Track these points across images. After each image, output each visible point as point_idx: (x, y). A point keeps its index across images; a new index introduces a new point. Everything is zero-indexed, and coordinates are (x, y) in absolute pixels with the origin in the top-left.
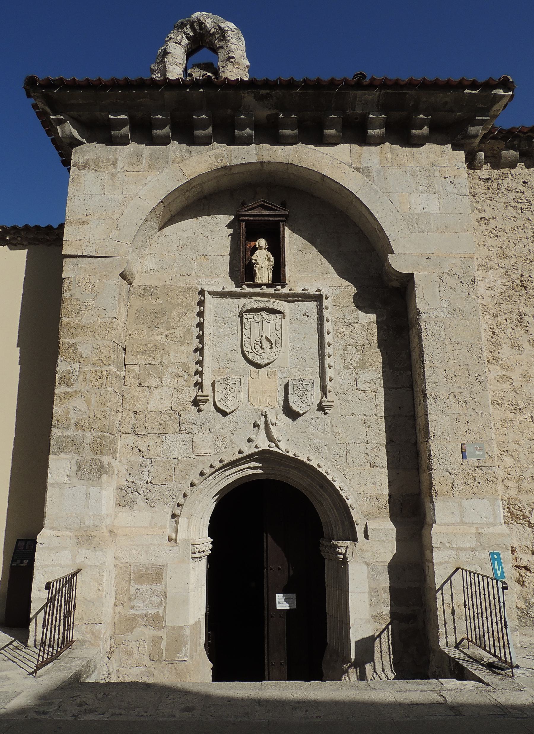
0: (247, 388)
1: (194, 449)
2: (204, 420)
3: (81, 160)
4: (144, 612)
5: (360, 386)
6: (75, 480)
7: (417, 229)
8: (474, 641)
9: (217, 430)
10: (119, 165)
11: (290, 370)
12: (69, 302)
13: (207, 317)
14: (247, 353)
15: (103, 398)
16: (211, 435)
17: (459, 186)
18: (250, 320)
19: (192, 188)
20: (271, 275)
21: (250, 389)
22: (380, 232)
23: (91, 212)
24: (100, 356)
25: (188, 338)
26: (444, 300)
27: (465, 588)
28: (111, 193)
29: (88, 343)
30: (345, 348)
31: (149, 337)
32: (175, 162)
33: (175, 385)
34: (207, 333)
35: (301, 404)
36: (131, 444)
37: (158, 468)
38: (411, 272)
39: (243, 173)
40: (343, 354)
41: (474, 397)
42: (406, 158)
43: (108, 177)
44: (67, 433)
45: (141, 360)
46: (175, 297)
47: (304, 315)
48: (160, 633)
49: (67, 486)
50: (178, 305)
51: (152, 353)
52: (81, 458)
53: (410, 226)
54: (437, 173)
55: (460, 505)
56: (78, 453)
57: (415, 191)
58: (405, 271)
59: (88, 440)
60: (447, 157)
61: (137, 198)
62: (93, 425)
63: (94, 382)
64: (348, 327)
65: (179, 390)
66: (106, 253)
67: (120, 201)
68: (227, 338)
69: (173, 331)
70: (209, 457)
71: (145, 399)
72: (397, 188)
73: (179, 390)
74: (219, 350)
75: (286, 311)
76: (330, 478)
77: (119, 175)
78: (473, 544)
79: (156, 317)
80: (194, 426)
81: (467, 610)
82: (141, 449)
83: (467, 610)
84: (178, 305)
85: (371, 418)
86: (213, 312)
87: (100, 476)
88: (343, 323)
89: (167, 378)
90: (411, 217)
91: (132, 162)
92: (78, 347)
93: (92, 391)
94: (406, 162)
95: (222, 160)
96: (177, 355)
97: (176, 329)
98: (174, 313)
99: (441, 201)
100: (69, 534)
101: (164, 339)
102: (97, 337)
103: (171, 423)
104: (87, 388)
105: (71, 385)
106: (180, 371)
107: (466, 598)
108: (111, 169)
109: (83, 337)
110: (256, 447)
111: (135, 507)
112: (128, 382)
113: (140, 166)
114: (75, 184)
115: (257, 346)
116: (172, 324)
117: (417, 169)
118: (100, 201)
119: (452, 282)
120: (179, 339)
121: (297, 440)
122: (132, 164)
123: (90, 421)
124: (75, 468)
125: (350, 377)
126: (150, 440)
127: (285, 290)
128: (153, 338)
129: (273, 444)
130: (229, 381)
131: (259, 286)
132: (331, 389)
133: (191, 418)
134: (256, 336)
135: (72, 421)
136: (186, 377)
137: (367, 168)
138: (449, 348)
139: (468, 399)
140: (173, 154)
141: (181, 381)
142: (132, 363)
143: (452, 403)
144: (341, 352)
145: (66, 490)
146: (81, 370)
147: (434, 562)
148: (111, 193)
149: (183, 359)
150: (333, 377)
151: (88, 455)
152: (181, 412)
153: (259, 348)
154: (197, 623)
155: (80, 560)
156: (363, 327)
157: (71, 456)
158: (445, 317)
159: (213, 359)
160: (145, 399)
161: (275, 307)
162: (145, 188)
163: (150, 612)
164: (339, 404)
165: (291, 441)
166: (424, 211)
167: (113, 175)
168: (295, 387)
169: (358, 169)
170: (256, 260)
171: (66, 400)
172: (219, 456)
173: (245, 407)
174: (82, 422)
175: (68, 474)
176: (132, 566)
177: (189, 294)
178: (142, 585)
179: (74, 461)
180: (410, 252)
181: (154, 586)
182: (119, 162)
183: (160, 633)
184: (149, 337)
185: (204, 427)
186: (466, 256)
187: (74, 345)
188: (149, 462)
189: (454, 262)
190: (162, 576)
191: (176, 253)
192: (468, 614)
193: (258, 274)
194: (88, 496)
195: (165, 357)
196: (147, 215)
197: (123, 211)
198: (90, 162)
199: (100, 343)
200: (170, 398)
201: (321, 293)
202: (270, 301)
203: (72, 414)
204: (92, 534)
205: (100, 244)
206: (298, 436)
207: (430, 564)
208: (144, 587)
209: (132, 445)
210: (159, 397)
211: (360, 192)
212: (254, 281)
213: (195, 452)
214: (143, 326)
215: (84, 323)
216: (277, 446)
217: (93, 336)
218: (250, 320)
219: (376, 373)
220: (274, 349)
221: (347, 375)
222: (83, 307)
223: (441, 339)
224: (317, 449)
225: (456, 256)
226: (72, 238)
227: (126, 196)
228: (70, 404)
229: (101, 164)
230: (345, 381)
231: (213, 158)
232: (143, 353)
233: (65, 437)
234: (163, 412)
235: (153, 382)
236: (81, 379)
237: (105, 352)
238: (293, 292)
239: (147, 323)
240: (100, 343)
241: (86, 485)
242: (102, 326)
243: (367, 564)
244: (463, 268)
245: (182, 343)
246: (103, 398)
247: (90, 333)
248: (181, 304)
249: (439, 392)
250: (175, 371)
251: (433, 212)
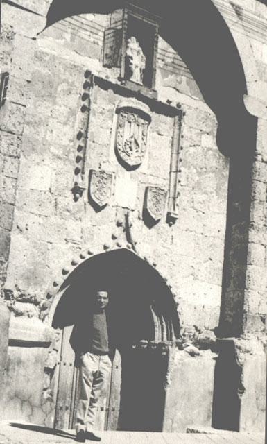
14: (119, 152)
38: (256, 115)
82: (20, 226)
110: (118, 245)
129: (130, 245)
134: (127, 137)
165: (147, 245)
216: (133, 248)
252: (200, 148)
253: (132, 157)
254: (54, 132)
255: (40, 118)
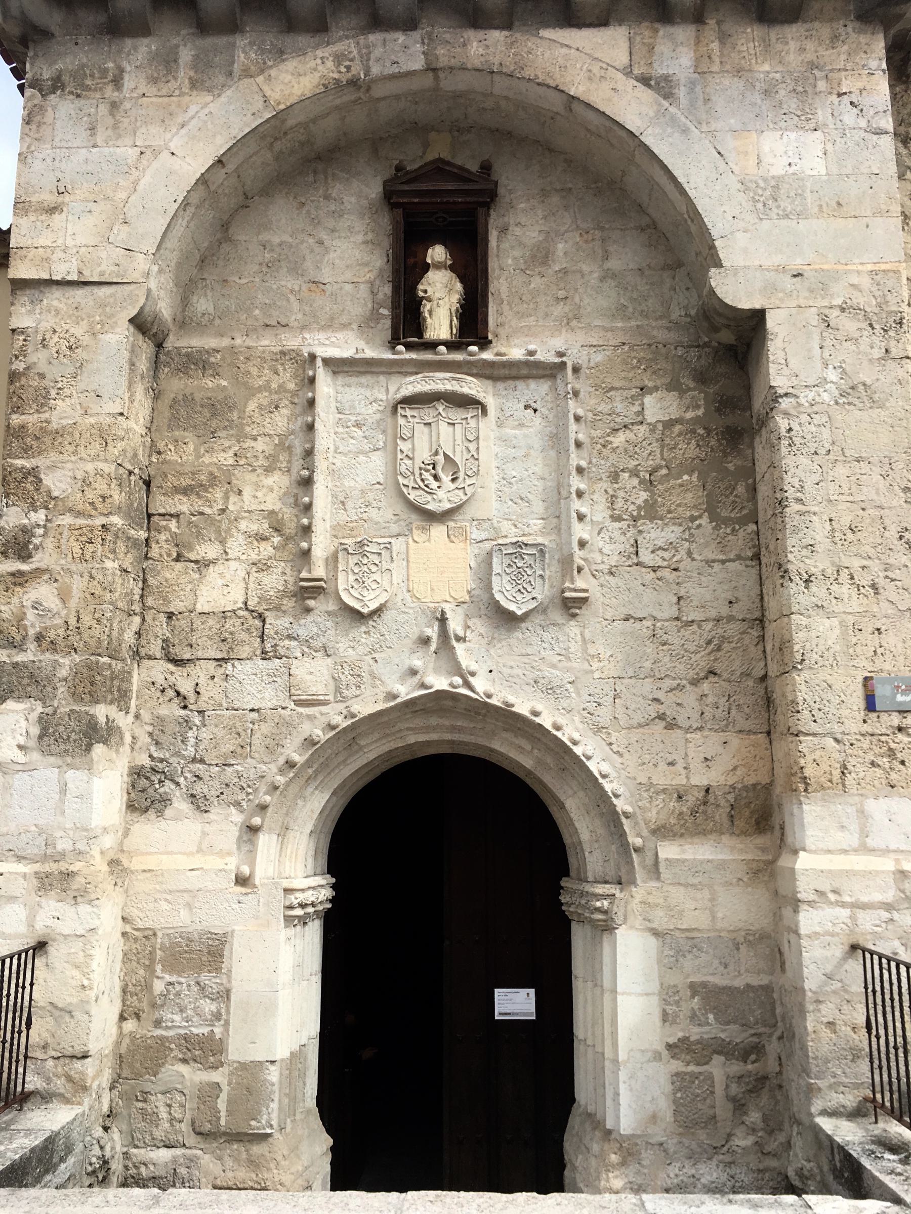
0: (405, 563)
1: (293, 691)
2: (315, 630)
3: (47, 74)
4: (182, 1032)
5: (646, 557)
6: (35, 756)
7: (775, 210)
8: (888, 1104)
9: (341, 650)
10: (128, 82)
11: (496, 525)
12: (23, 381)
13: (322, 414)
14: (405, 490)
15: (96, 583)
16: (329, 661)
17: (872, 112)
18: (410, 419)
19: (285, 133)
20: (455, 321)
21: (411, 565)
22: (692, 221)
23: (69, 187)
24: (90, 495)
25: (281, 458)
26: (831, 367)
27: (870, 990)
28: (111, 143)
29: (63, 468)
30: (615, 477)
31: (198, 456)
32: (247, 73)
33: (254, 557)
34: (321, 448)
35: (519, 597)
36: (160, 680)
37: (216, 730)
38: (758, 307)
39: (397, 97)
40: (609, 490)
41: (894, 576)
42: (753, 52)
43: (103, 109)
44: (20, 658)
45: (183, 505)
46: (254, 371)
47: (526, 407)
48: (216, 1076)
49: (19, 767)
50: (260, 389)
51: (206, 491)
52: (49, 710)
53: (760, 206)
54: (822, 85)
55: (861, 812)
56: (43, 700)
57: (771, 126)
58: (745, 304)
59: (63, 672)
60: (846, 47)
61: (166, 154)
62: (74, 640)
63: (77, 550)
64: (621, 433)
65: (261, 566)
66: (102, 274)
67: (129, 161)
68: (362, 458)
69: (249, 443)
70: (323, 709)
71: (190, 586)
72: (732, 121)
73: (261, 566)
74: (347, 484)
75: (490, 401)
76: (578, 750)
77: (127, 105)
78: (889, 896)
79: (214, 415)
80: (294, 643)
81: (874, 1039)
82: (182, 690)
83: (874, 1039)
84: (260, 389)
85: (666, 624)
86: (333, 405)
87: (89, 748)
88: (612, 425)
89: (236, 545)
90: (762, 184)
91: (155, 75)
92: (42, 476)
93: (73, 568)
94: (754, 61)
95: (348, 68)
96: (259, 494)
97: (256, 440)
98: (252, 406)
99: (829, 147)
100: (21, 868)
101: (231, 461)
102: (85, 457)
103: (244, 636)
104: (63, 562)
105: (30, 556)
106: (264, 527)
107: (872, 1012)
108: (109, 91)
109: (53, 456)
110: (423, 686)
111: (168, 812)
112: (155, 551)
113: (173, 84)
114: (34, 127)
115: (426, 475)
116: (248, 429)
117: (778, 76)
118: (86, 161)
119: (849, 325)
120: (262, 461)
121: (509, 671)
122: (154, 80)
123: (69, 632)
124: (35, 731)
125: (623, 539)
126: (201, 672)
127: (487, 355)
128: (207, 459)
129: (458, 680)
130: (366, 548)
131: (432, 346)
132: (582, 563)
133: (287, 625)
134: (423, 454)
135: (32, 632)
136: (277, 540)
137: (666, 78)
138: (841, 471)
139: (881, 582)
140: (242, 55)
141: (267, 549)
142: (162, 511)
143: (845, 590)
144: (605, 485)
145: (17, 776)
146: (49, 525)
147: (803, 931)
148: (111, 143)
149: (272, 502)
150: (586, 536)
151: (63, 703)
152: (267, 613)
153: (431, 478)
154: (297, 1056)
155: (43, 923)
156: (653, 430)
157: (28, 705)
158: (832, 403)
159: (334, 504)
160: (190, 586)
161: (466, 390)
162: (183, 131)
163: (195, 1031)
164: (599, 595)
166: (791, 170)
167: (114, 106)
168: (507, 561)
169: (645, 81)
170: (425, 292)
171: (18, 589)
172: (345, 705)
173: (400, 603)
174: (52, 635)
175: (22, 743)
176: (159, 934)
177: (282, 364)
178: (179, 973)
179: (34, 716)
180: (757, 263)
181: (205, 978)
182: (126, 77)
183: (216, 1076)
184: (198, 456)
185: (314, 644)
186: (883, 267)
187: (34, 473)
188: (197, 720)
189: (855, 280)
190: (222, 956)
191: (257, 279)
192: (875, 1046)
193: (429, 321)
194: (64, 791)
195: (233, 498)
196: (188, 192)
197: (136, 183)
198: (66, 78)
199: (90, 467)
200: (243, 585)
201: (564, 359)
202: (454, 379)
203: (31, 615)
204: (72, 868)
205: (89, 256)
206: (512, 663)
207: (792, 937)
208: (183, 980)
209: (163, 682)
210: (220, 582)
211: (650, 131)
212: (420, 334)
213: (295, 698)
214: (186, 434)
215: (54, 425)
217: (75, 453)
218: (410, 419)
219: (682, 529)
220: (461, 479)
221: (617, 534)
222: (53, 393)
223: (822, 451)
224: (550, 690)
225: (860, 268)
226: (30, 242)
227: (143, 149)
228: (26, 597)
229: (88, 82)
230: (613, 547)
231: (330, 64)
232: (185, 491)
233: (16, 665)
234: (229, 614)
235: (208, 550)
236: (49, 543)
237: (101, 486)
238: (504, 358)
239: (194, 427)
240: (90, 467)
241: (59, 767)
242: (94, 431)
243: (656, 933)
244: (877, 294)
245: (268, 470)
246: (96, 583)
247: (68, 447)
248: (267, 387)
249: (815, 567)
250: (254, 527)
251: (812, 173)
252: (643, 428)
253: (441, 494)
254: (244, 493)
255: (211, 474)
